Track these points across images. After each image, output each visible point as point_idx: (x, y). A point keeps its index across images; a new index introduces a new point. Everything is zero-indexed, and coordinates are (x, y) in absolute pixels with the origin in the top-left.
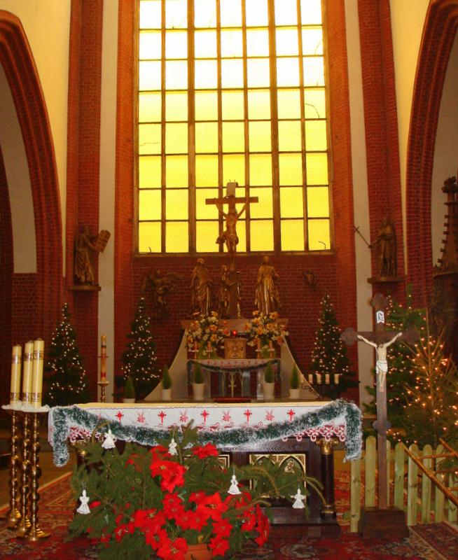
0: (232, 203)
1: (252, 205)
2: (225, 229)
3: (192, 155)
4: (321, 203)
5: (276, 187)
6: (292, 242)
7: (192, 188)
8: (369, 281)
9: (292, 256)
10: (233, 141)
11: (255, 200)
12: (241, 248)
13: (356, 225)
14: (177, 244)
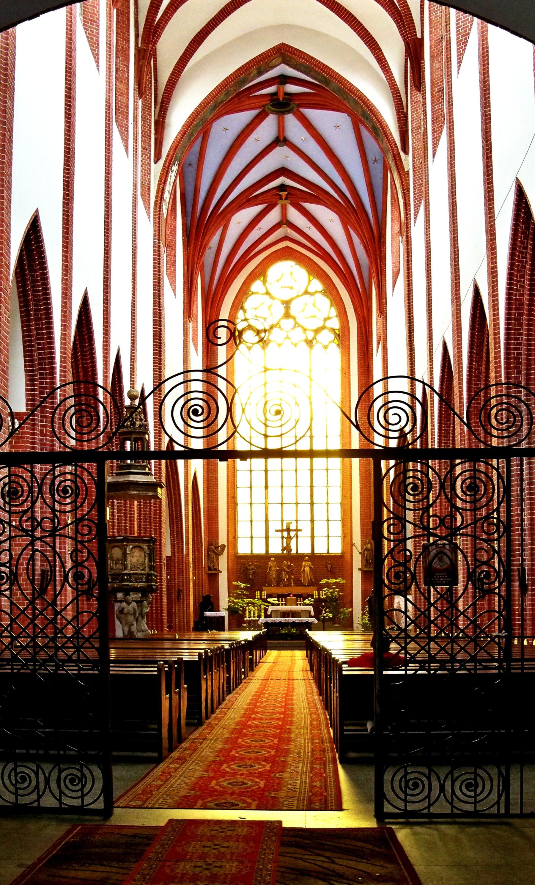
0: (288, 532)
2: (285, 545)
6: (321, 549)
9: (321, 557)
11: (301, 530)
12: (294, 552)
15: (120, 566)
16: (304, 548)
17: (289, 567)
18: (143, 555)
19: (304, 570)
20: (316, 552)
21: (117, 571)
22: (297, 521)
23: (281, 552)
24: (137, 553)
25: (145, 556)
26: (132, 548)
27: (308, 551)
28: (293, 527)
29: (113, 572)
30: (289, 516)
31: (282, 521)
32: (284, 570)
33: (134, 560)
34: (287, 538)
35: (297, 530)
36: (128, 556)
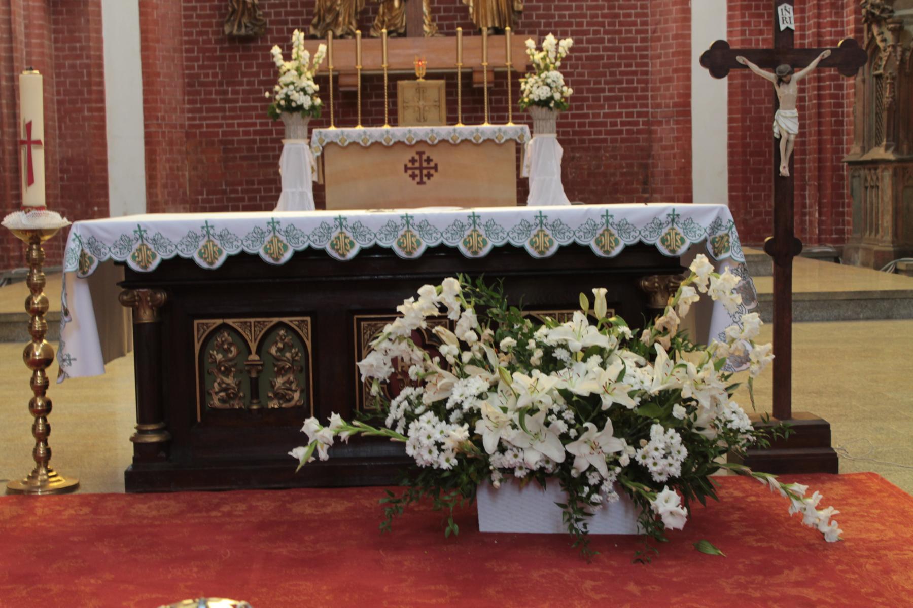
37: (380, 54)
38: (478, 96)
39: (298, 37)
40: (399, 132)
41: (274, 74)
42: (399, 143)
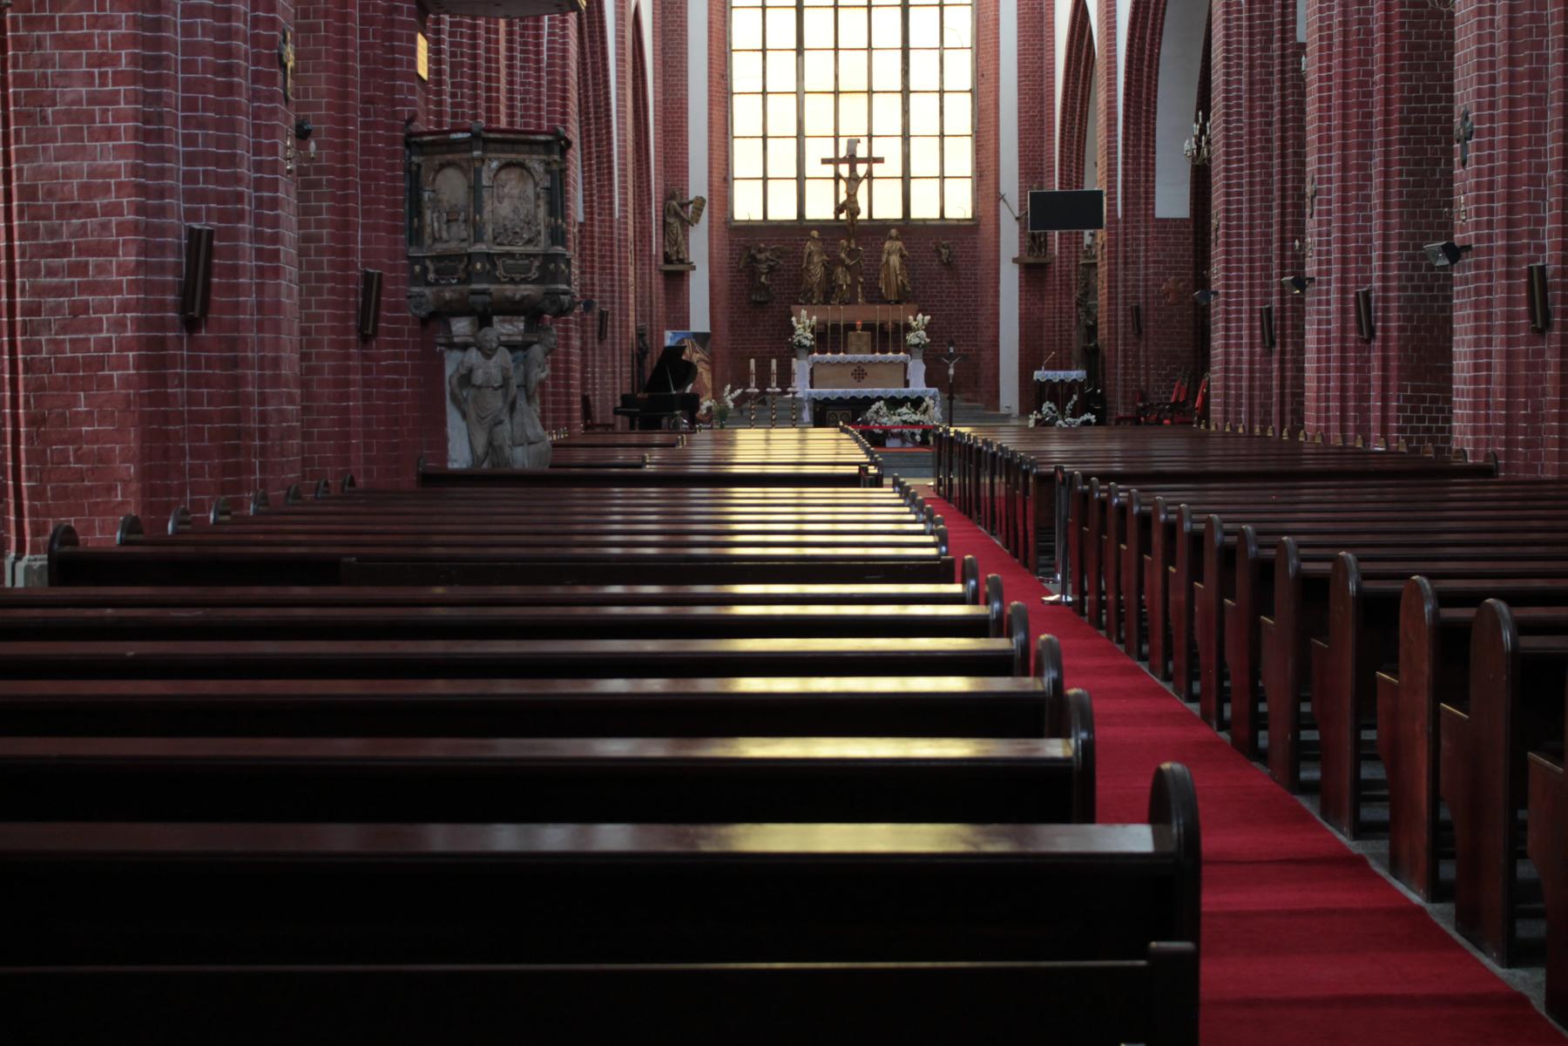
1: (875, 166)
2: (843, 197)
3: (800, 93)
4: (961, 157)
5: (906, 137)
7: (800, 136)
8: (1015, 261)
9: (924, 226)
10: (853, 75)
11: (881, 160)
12: (863, 215)
13: (1002, 191)
14: (783, 209)
15: (460, 230)
16: (885, 205)
17: (851, 253)
18: (530, 192)
19: (888, 262)
20: (915, 214)
21: (453, 246)
22: (870, 136)
23: (832, 217)
24: (512, 184)
25: (538, 197)
26: (500, 169)
27: (896, 213)
28: (862, 152)
29: (439, 248)
30: (853, 124)
31: (836, 137)
32: (842, 262)
33: (505, 209)
34: (848, 180)
35: (871, 160)
36: (486, 194)
37: (839, 314)
38: (888, 337)
39: (804, 312)
40: (849, 357)
41: (792, 329)
42: (849, 363)
